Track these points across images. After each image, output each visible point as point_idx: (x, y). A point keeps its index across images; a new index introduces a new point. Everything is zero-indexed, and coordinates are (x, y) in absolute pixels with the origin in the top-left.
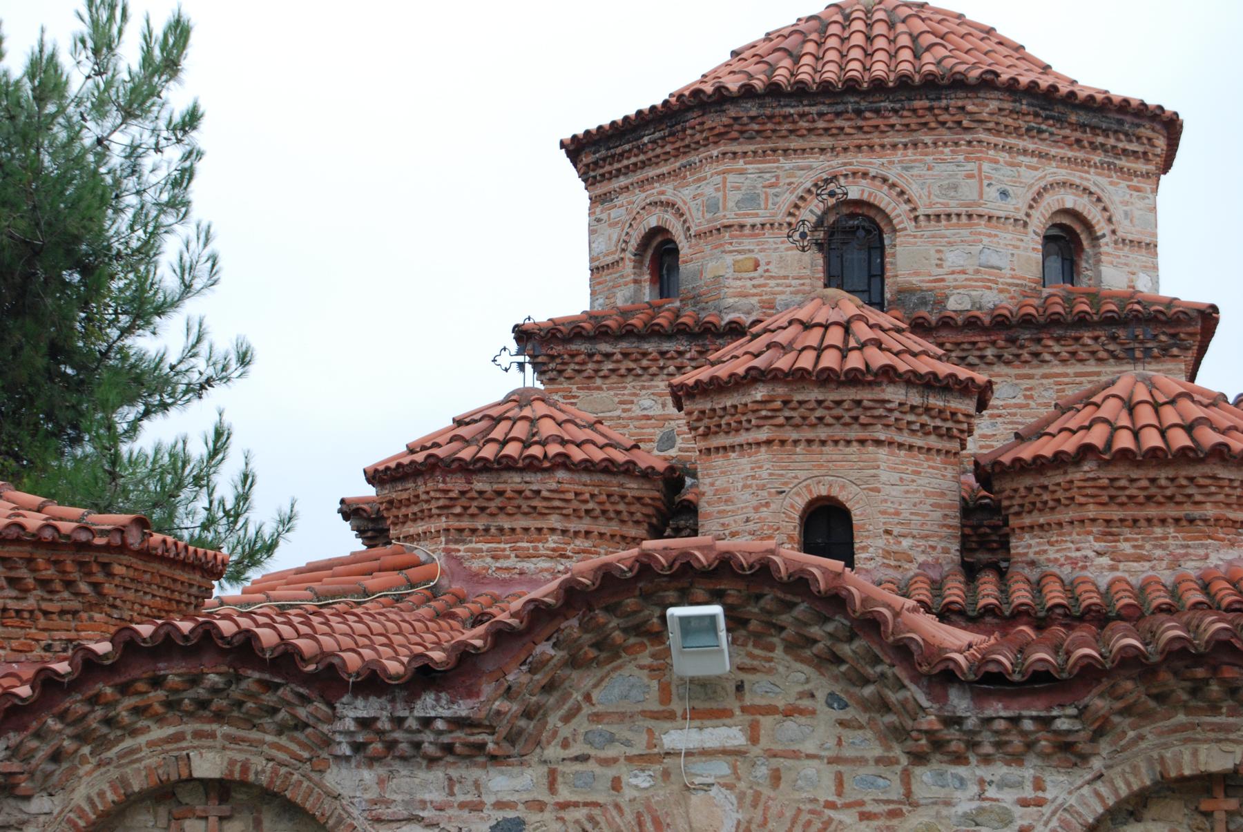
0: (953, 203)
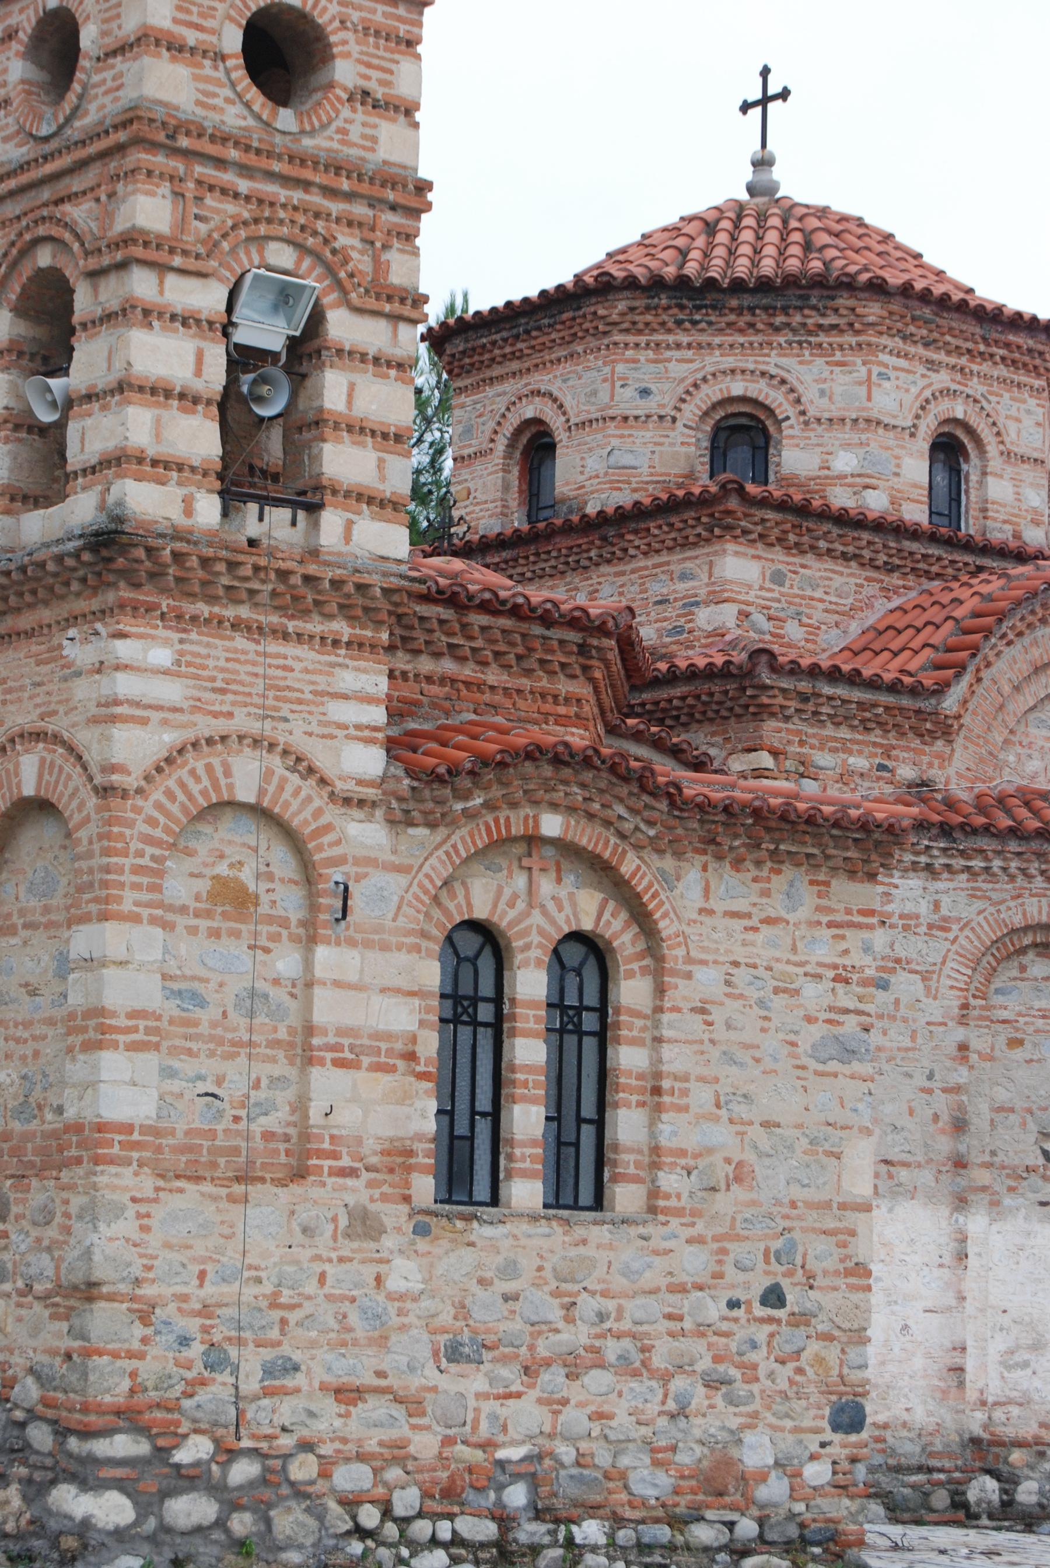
0: (593, 409)
